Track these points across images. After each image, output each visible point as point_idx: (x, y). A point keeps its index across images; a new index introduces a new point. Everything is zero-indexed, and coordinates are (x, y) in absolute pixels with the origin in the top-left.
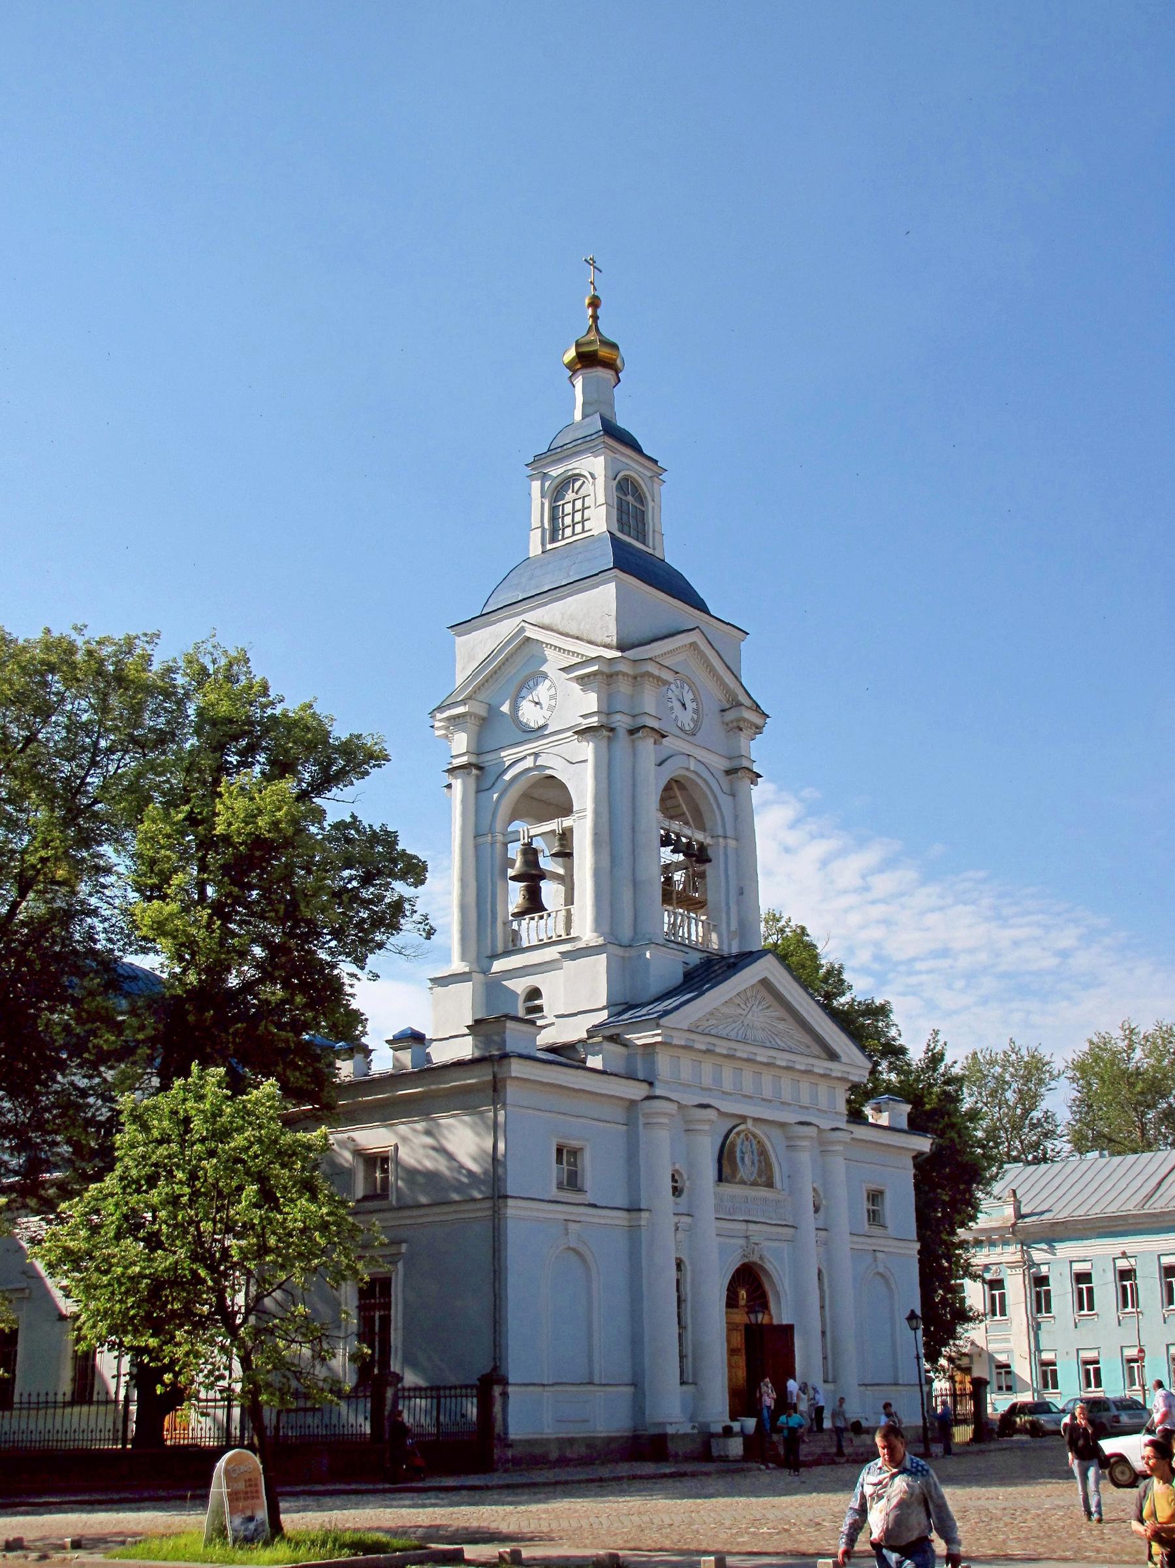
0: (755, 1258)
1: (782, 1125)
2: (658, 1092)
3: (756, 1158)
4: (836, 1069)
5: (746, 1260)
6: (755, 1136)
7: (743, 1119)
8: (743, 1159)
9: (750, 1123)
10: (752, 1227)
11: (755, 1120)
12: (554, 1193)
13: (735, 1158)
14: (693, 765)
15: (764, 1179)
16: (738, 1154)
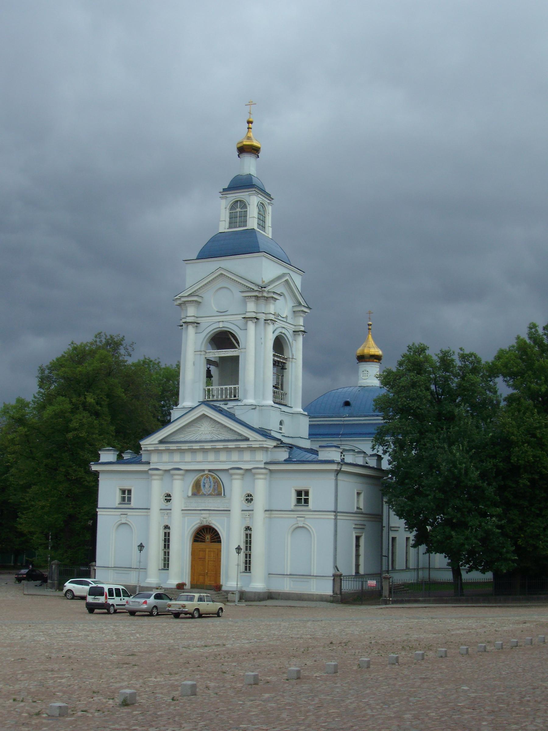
0: (205, 523)
1: (227, 470)
2: (151, 467)
3: (212, 484)
4: (243, 444)
5: (202, 525)
6: (212, 476)
7: (203, 471)
8: (204, 486)
9: (206, 472)
10: (203, 512)
11: (210, 471)
12: (117, 505)
13: (200, 486)
14: (221, 325)
15: (216, 492)
16: (202, 484)
